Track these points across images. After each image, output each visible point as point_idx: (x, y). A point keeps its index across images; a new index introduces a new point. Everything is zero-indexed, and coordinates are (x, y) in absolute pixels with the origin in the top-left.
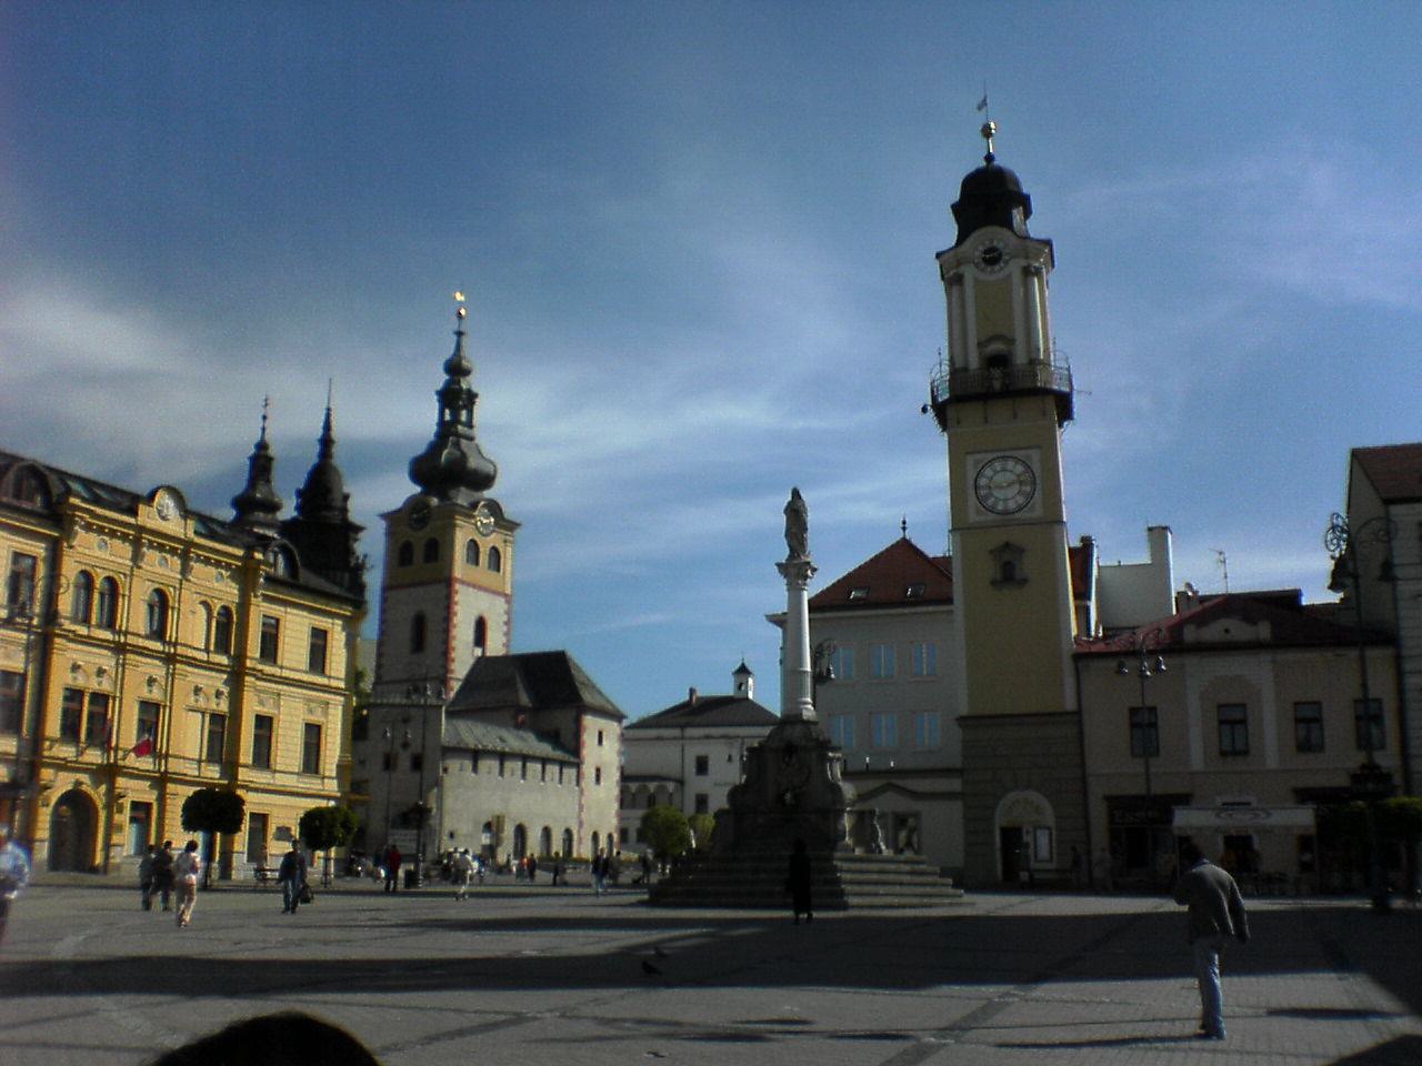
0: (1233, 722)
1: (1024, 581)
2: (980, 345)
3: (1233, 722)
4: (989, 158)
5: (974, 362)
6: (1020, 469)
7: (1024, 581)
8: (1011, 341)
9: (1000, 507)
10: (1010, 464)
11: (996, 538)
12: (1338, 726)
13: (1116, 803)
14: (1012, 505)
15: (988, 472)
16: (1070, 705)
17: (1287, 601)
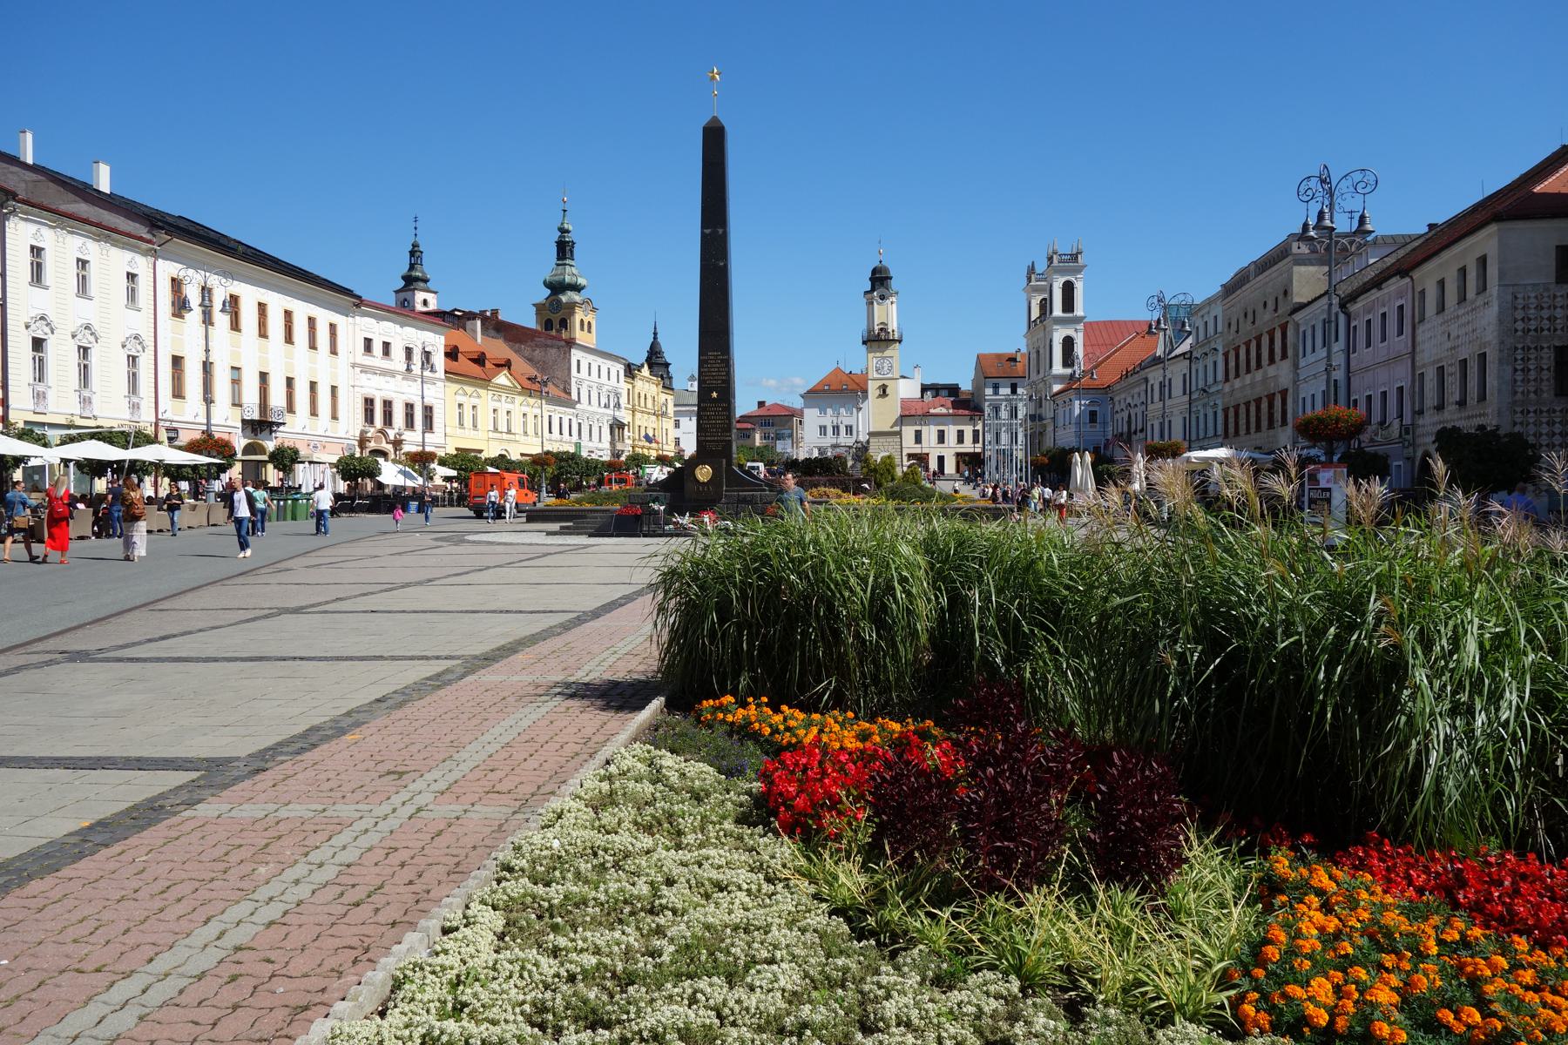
0: (941, 437)
3: (941, 437)
12: (968, 437)
17: (953, 390)
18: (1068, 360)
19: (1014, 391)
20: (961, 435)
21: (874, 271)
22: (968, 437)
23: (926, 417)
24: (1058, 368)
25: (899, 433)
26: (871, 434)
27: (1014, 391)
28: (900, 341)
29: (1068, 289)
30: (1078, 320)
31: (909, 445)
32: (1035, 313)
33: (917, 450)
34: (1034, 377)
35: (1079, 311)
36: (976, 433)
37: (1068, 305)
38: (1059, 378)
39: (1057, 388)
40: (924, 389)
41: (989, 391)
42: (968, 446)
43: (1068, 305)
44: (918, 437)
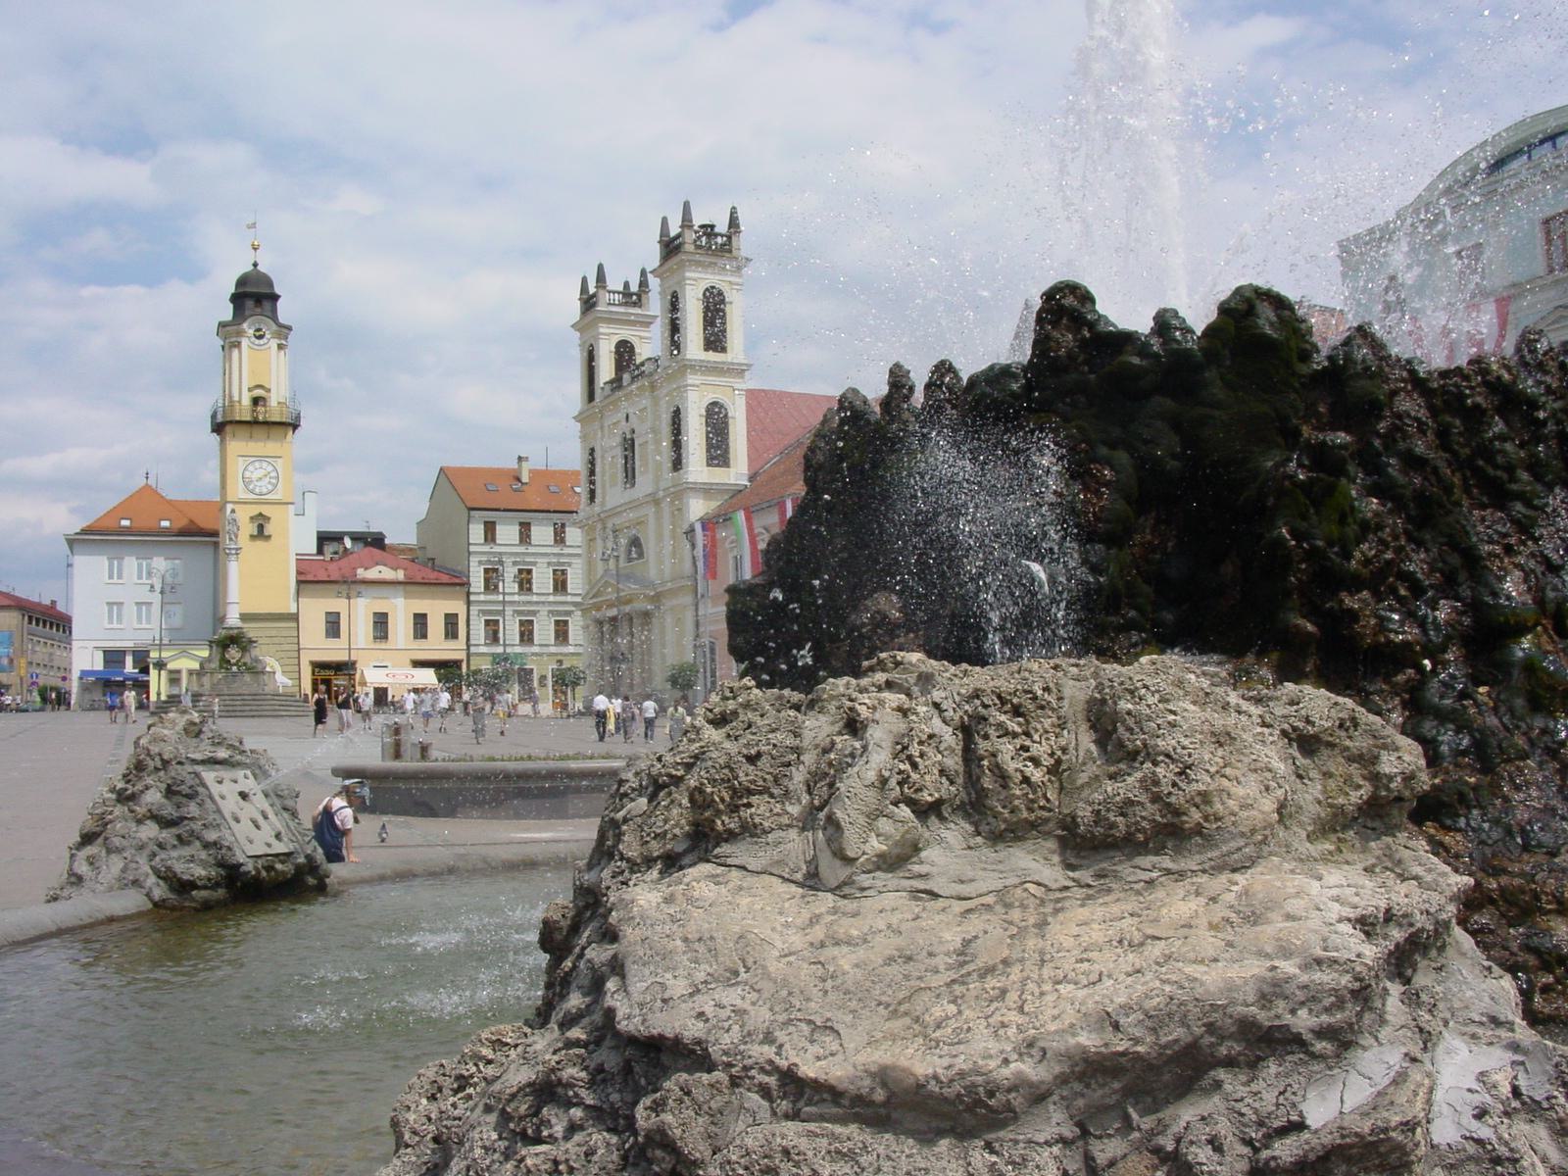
0: (381, 623)
1: (269, 537)
2: (250, 390)
3: (381, 623)
4: (255, 265)
5: (246, 401)
6: (270, 468)
7: (269, 537)
8: (269, 391)
9: (257, 490)
10: (265, 465)
11: (255, 510)
12: (436, 626)
13: (318, 666)
14: (265, 491)
15: (251, 468)
16: (293, 610)
17: (376, 541)
18: (718, 452)
19: (525, 537)
20: (420, 623)
21: (242, 282)
22: (436, 626)
23: (349, 585)
24: (696, 468)
25: (294, 618)
26: (244, 617)
27: (525, 537)
28: (295, 427)
29: (715, 307)
30: (739, 371)
31: (318, 646)
32: (606, 370)
33: (333, 651)
34: (613, 494)
35: (737, 348)
36: (451, 621)
37: (715, 341)
38: (707, 490)
39: (698, 508)
40: (324, 539)
41: (477, 532)
42: (436, 646)
43: (715, 341)
44: (333, 626)
